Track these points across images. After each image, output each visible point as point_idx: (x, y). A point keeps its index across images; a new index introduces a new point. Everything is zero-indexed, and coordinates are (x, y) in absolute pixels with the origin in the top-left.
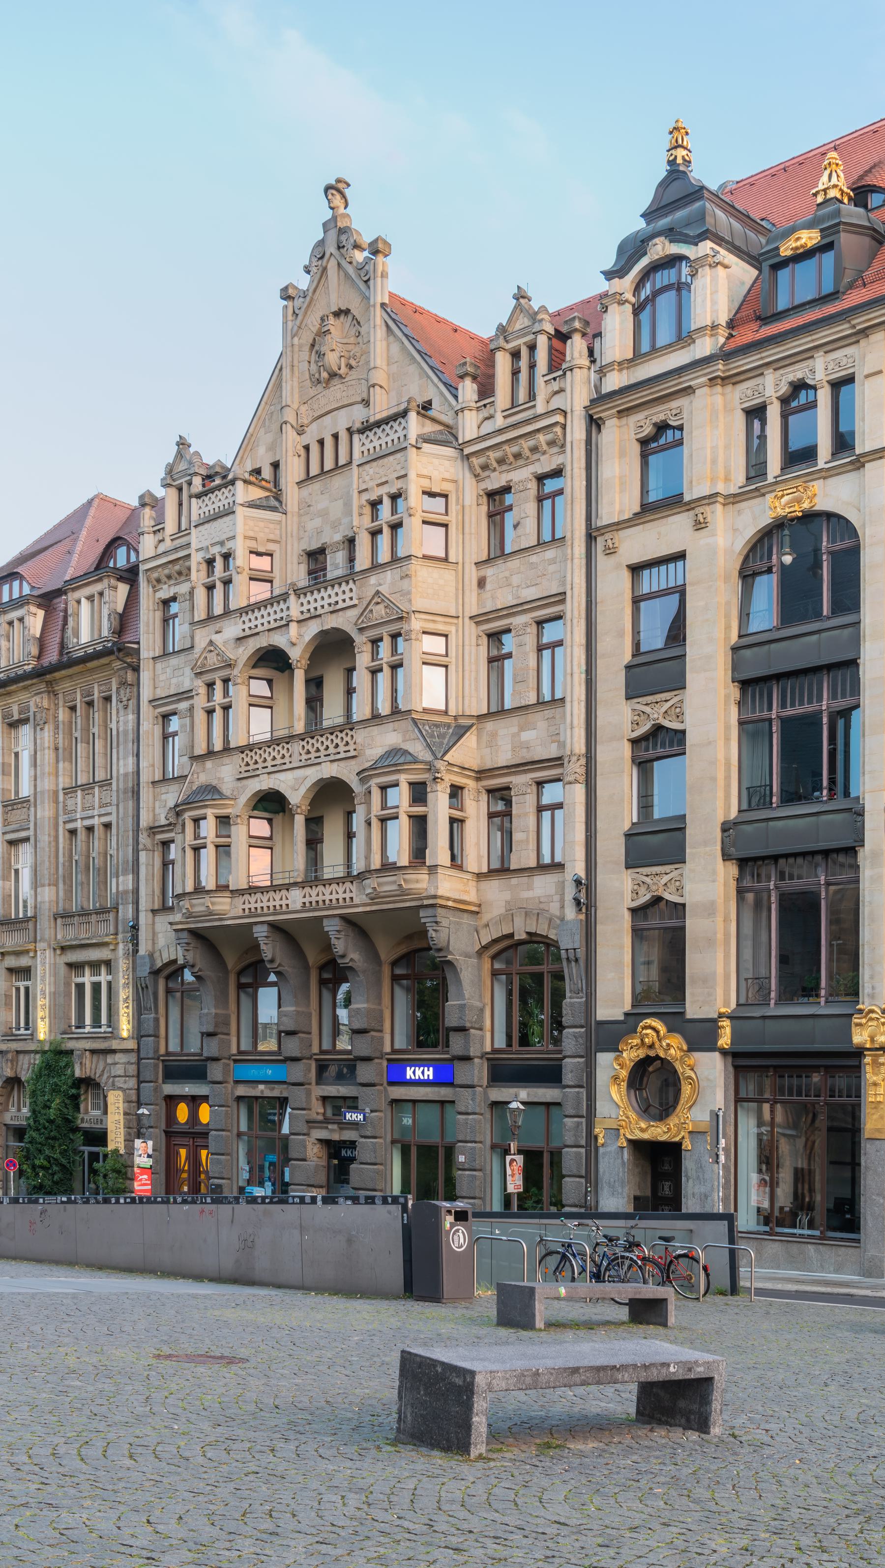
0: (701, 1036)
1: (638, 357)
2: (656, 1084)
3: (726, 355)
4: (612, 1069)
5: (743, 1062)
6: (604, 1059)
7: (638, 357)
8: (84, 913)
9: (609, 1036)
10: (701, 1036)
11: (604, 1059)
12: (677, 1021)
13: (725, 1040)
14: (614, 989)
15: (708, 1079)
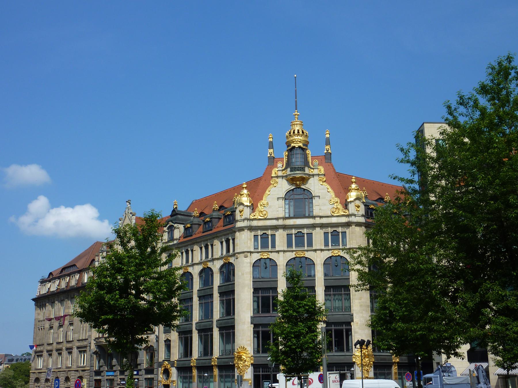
0: (172, 364)
1: (168, 242)
2: (167, 372)
3: (178, 244)
4: (161, 370)
5: (179, 369)
6: (160, 369)
7: (168, 242)
8: (82, 340)
9: (160, 365)
10: (172, 364)
11: (160, 369)
12: (169, 361)
13: (176, 365)
14: (162, 355)
15: (174, 371)
